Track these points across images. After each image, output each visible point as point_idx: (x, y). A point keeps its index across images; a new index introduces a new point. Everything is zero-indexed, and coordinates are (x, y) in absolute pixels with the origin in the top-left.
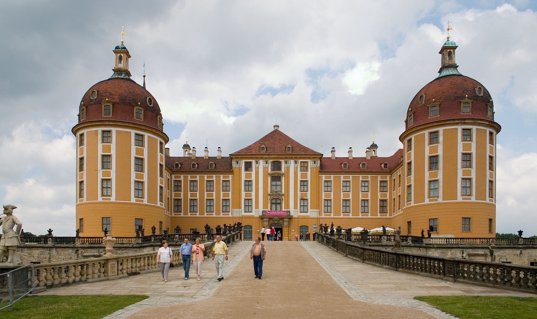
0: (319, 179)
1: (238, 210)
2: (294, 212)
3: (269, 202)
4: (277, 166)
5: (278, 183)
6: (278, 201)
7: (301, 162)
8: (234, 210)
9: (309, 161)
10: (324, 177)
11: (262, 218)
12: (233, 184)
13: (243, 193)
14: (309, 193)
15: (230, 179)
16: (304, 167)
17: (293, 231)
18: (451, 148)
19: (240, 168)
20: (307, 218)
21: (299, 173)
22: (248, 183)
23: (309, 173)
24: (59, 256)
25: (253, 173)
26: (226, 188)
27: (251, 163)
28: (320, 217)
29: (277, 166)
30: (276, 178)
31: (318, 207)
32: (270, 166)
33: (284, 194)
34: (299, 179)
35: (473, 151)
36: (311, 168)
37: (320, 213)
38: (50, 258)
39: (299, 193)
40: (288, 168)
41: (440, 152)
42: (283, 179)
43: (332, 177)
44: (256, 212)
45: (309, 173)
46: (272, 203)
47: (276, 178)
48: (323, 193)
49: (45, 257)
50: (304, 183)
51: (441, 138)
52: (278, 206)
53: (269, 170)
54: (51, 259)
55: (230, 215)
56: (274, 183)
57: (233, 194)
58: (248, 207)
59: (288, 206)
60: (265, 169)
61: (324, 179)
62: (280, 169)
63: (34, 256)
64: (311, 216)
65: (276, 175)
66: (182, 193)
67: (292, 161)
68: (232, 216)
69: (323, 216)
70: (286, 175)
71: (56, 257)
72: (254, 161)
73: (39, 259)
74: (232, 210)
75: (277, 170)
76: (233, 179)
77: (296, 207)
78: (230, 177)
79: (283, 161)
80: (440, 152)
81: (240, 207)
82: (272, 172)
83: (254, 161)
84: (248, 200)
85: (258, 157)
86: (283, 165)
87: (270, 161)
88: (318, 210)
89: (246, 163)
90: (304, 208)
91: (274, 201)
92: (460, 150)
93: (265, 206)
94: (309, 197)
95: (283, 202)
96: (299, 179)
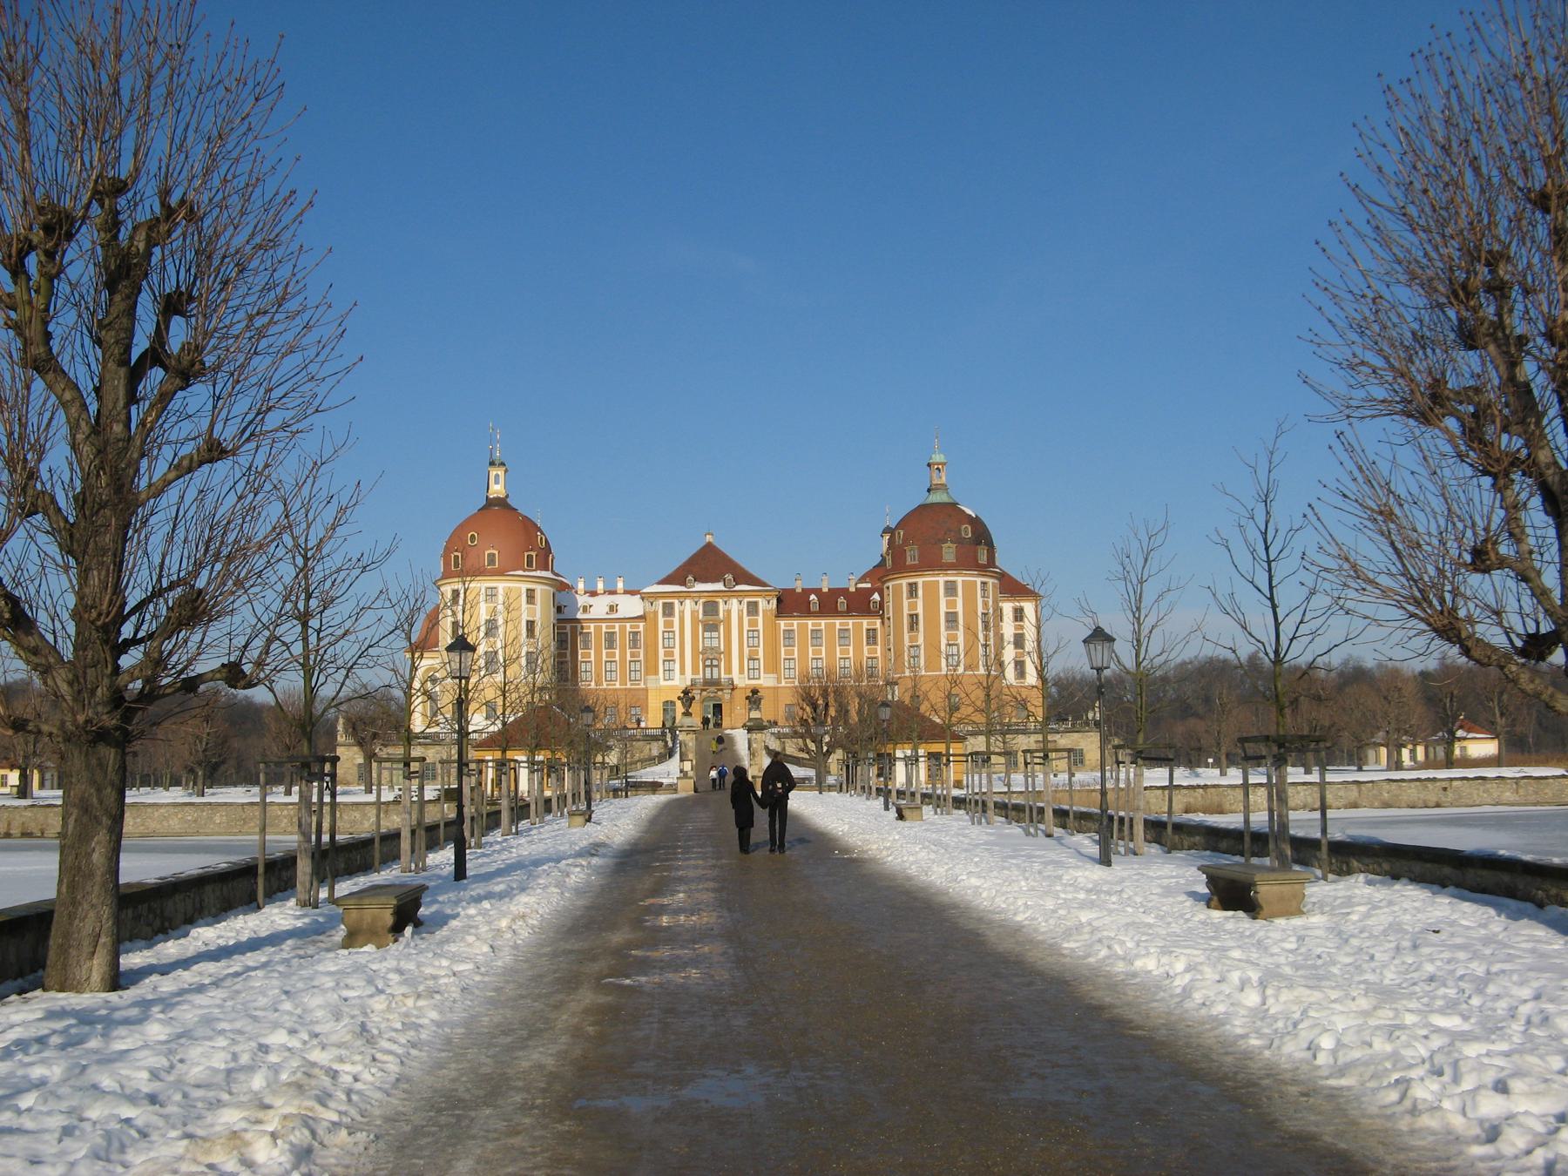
0: (776, 628)
2: (741, 680)
4: (710, 608)
5: (715, 634)
6: (715, 662)
9: (760, 600)
14: (761, 650)
15: (641, 629)
16: (753, 609)
18: (932, 605)
19: (656, 613)
21: (746, 619)
23: (760, 619)
27: (672, 604)
34: (746, 627)
35: (960, 609)
37: (779, 681)
39: (746, 650)
40: (729, 612)
41: (920, 610)
45: (760, 619)
46: (705, 666)
48: (783, 649)
51: (920, 592)
52: (715, 670)
53: (701, 616)
56: (707, 634)
59: (729, 670)
60: (694, 613)
61: (783, 627)
62: (716, 613)
64: (765, 685)
66: (568, 652)
67: (735, 601)
69: (783, 684)
72: (676, 602)
76: (645, 629)
77: (741, 671)
80: (920, 610)
81: (656, 673)
86: (721, 607)
89: (664, 604)
91: (708, 663)
92: (943, 609)
93: (695, 670)
94: (761, 655)
96: (746, 627)
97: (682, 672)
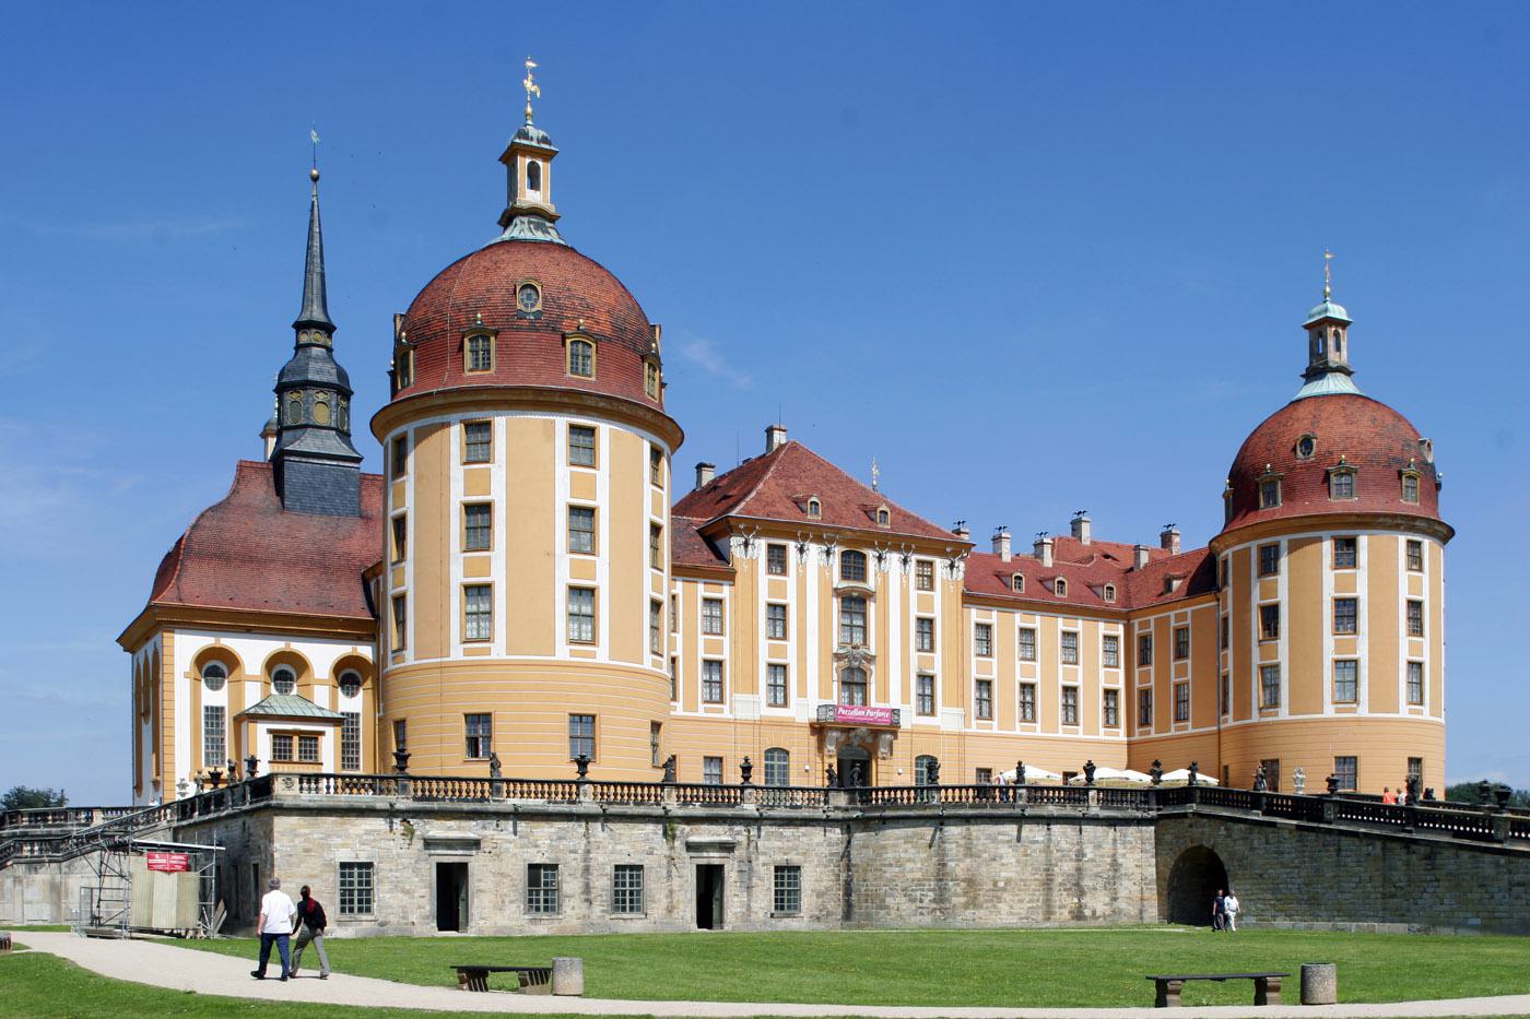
0: (963, 619)
1: (749, 697)
3: (835, 677)
4: (854, 566)
7: (919, 562)
8: (739, 697)
10: (975, 615)
11: (819, 729)
12: (735, 612)
13: (764, 644)
17: (900, 771)
19: (754, 562)
20: (934, 733)
21: (914, 594)
22: (778, 611)
24: (616, 844)
25: (791, 580)
26: (714, 626)
27: (784, 548)
28: (967, 730)
29: (854, 566)
30: (855, 603)
31: (961, 701)
32: (836, 561)
33: (875, 657)
36: (943, 580)
37: (967, 724)
38: (588, 852)
40: (885, 576)
42: (872, 607)
43: (993, 617)
44: (805, 707)
47: (855, 603)
48: (974, 659)
49: (572, 848)
50: (926, 624)
53: (837, 581)
54: (591, 855)
55: (727, 715)
57: (734, 643)
58: (779, 690)
59: (885, 696)
60: (823, 571)
62: (861, 574)
63: (539, 842)
64: (944, 729)
65: (855, 594)
67: (894, 558)
68: (731, 716)
69: (974, 729)
70: (879, 596)
71: (605, 848)
73: (553, 856)
74: (731, 695)
75: (855, 579)
78: (725, 592)
79: (871, 554)
81: (754, 690)
82: (845, 584)
83: (792, 546)
84: (777, 669)
85: (805, 533)
86: (872, 564)
87: (838, 550)
88: (961, 710)
90: (927, 703)
93: (824, 691)
95: (873, 679)
97: (802, 693)
